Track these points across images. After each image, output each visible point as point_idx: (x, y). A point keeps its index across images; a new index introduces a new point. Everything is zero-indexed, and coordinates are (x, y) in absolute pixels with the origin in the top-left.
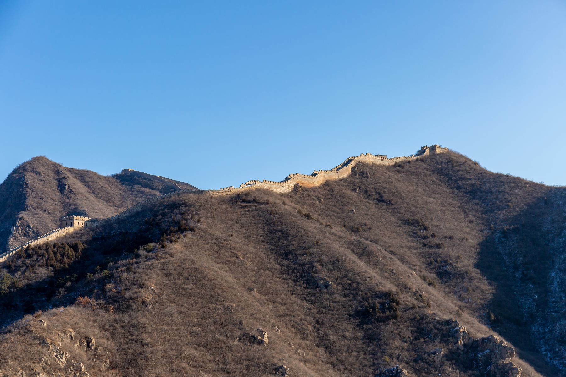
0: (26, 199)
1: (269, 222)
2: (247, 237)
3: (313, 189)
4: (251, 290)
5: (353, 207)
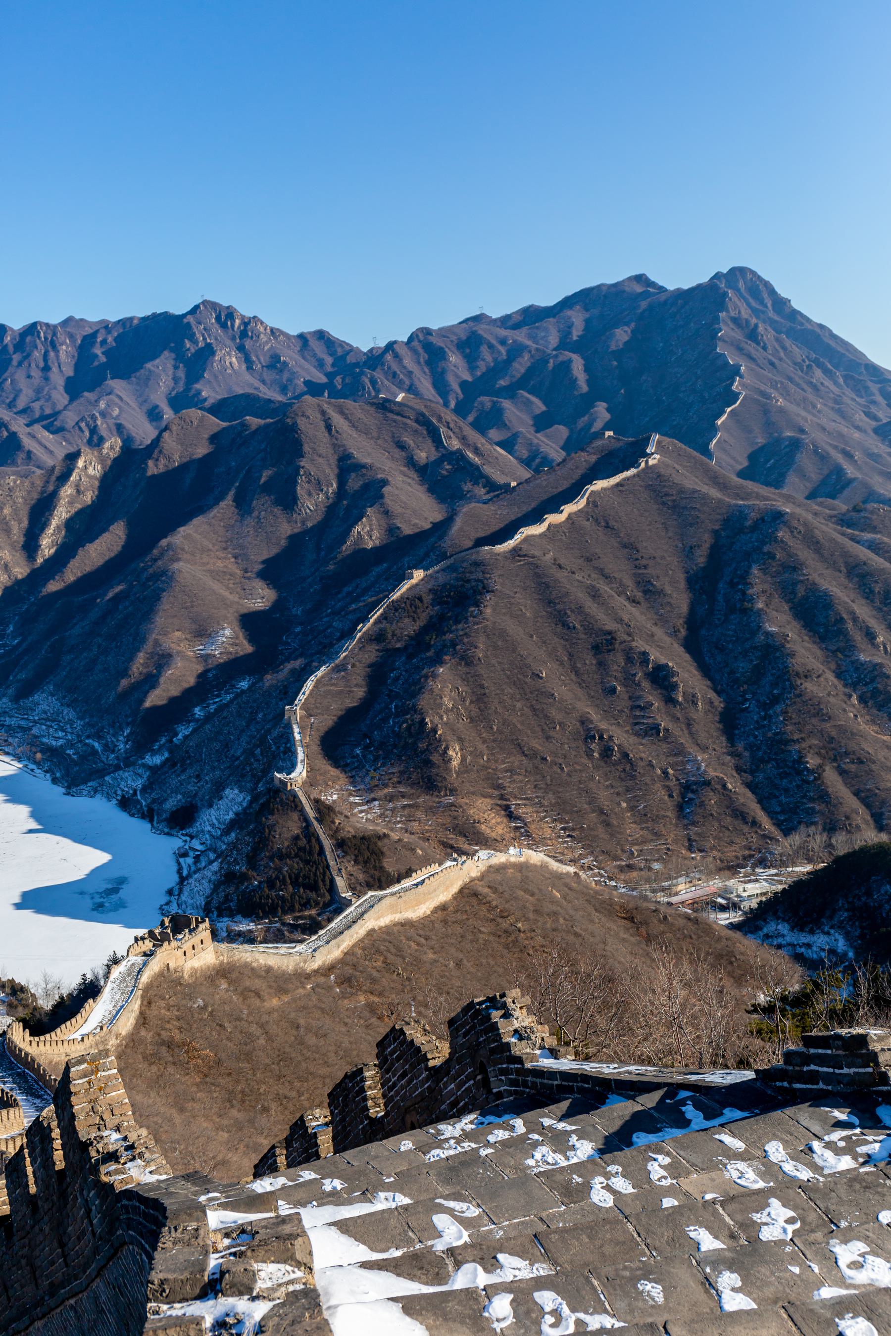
1: (537, 575)
3: (560, 525)
4: (532, 636)
5: (587, 538)
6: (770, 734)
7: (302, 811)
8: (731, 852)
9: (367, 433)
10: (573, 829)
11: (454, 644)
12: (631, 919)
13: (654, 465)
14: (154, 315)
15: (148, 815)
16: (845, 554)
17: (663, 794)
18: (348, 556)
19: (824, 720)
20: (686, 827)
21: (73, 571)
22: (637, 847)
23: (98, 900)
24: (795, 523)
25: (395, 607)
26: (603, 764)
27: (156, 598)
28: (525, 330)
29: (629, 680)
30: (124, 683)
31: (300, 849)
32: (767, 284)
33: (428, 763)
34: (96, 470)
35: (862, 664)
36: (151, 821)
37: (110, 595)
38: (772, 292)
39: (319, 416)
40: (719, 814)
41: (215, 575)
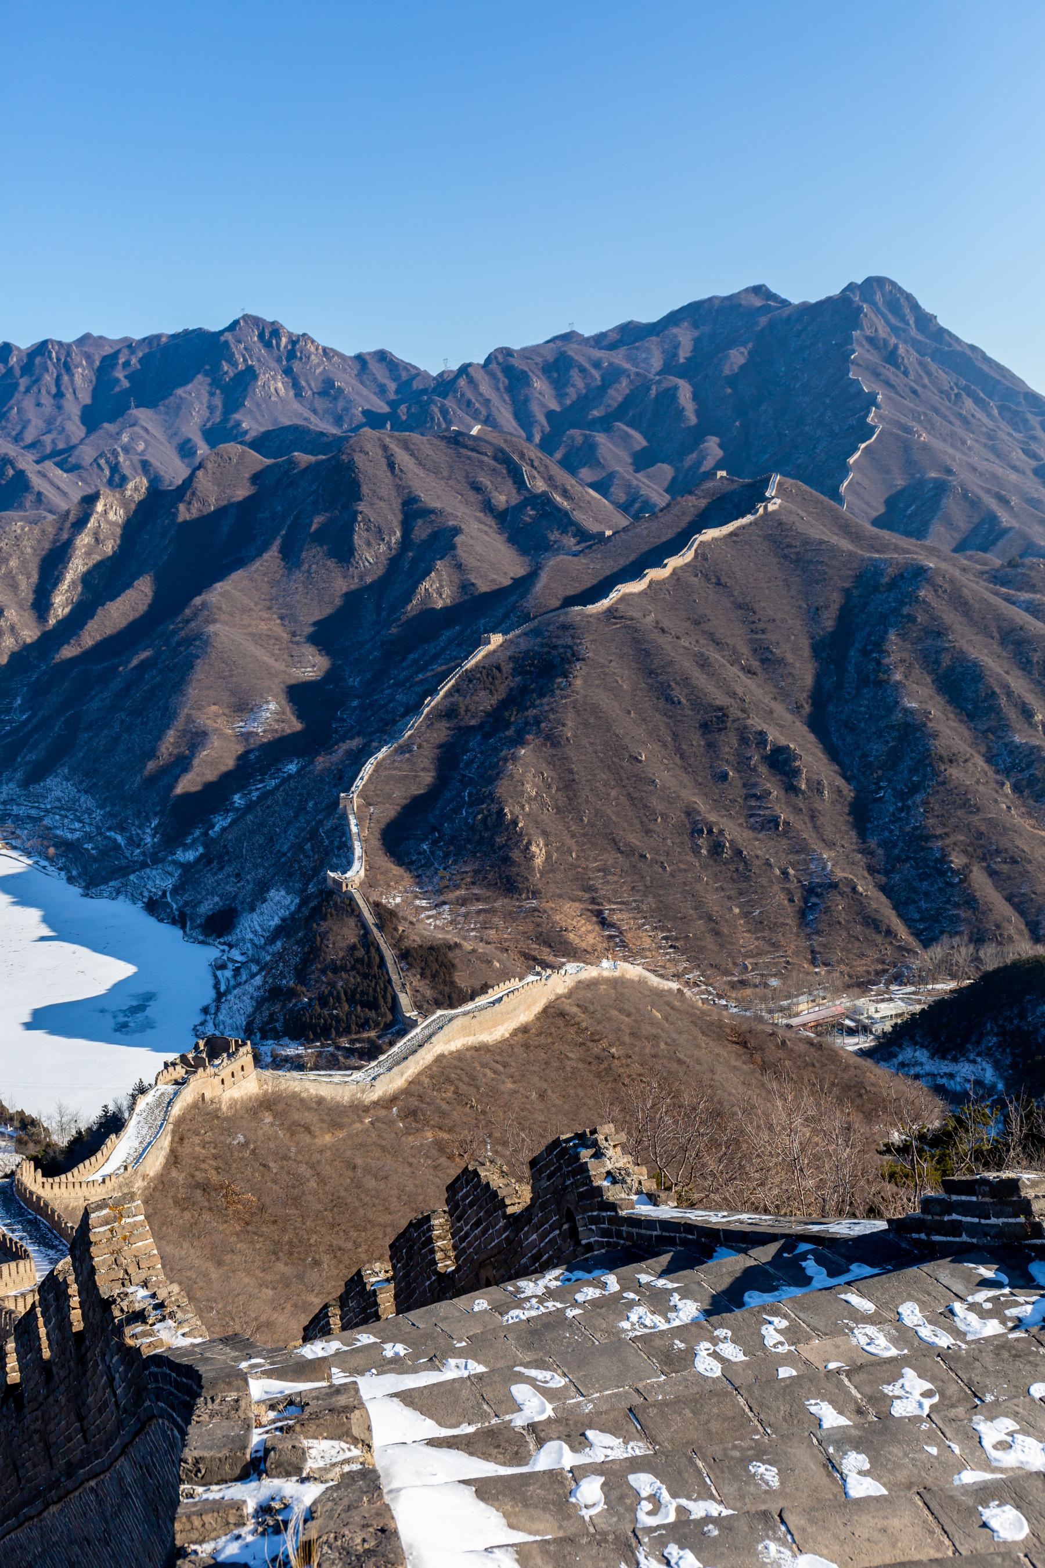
0: (359, 486)
1: (636, 641)
2: (621, 657)
4: (629, 712)
5: (695, 597)
6: (908, 829)
7: (359, 916)
8: (861, 967)
9: (436, 471)
10: (677, 939)
11: (538, 722)
12: (744, 1044)
13: (774, 512)
14: (186, 332)
15: (180, 920)
16: (999, 617)
17: (782, 898)
18: (414, 617)
19: (971, 812)
20: (809, 937)
21: (91, 635)
22: (751, 960)
23: (122, 1019)
24: (939, 580)
25: (469, 677)
26: (712, 862)
27: (189, 665)
28: (623, 350)
29: (743, 764)
30: (151, 765)
31: (357, 960)
32: (909, 298)
33: (507, 860)
34: (117, 516)
35: (1017, 747)
36: (183, 927)
37: (135, 662)
38: (915, 306)
39: (380, 452)
40: (847, 921)
41: (258, 639)
